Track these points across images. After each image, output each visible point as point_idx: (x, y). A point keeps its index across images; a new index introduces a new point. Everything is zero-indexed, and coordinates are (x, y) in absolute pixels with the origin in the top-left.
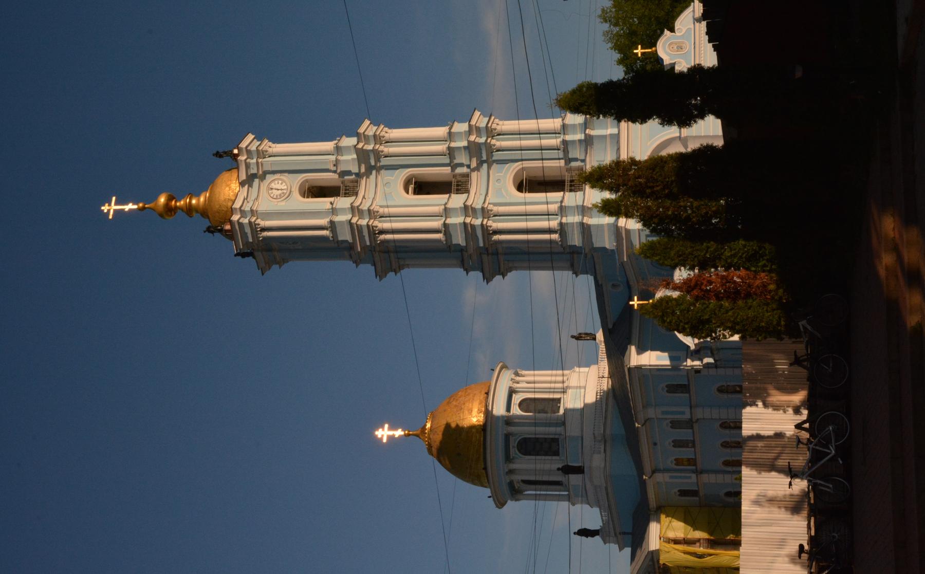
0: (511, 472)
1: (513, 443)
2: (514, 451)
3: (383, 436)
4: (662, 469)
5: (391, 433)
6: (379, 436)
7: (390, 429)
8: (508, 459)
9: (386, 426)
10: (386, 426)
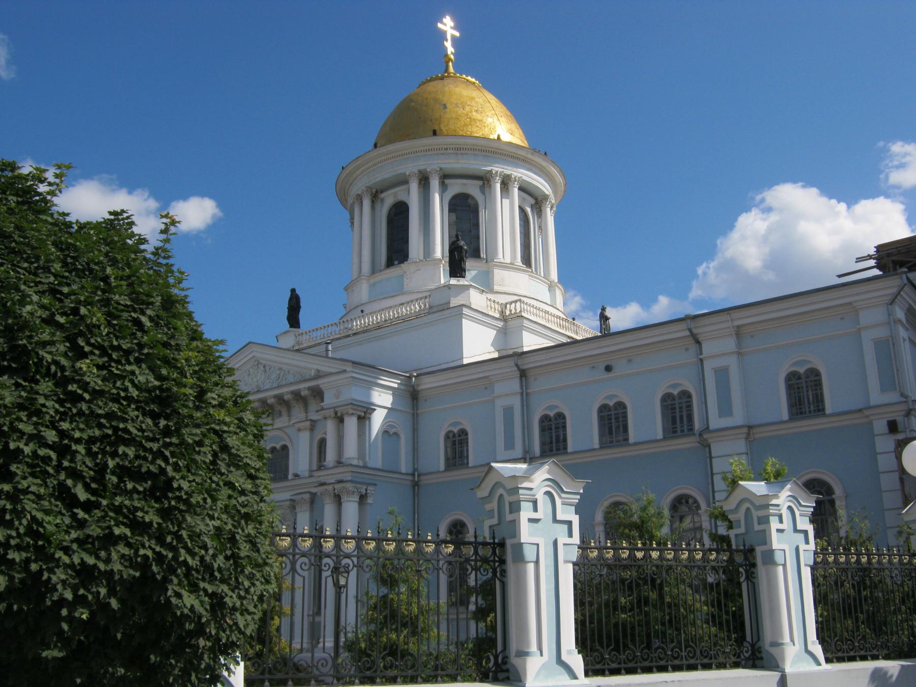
0: (424, 180)
1: (472, 187)
2: (456, 187)
3: (445, 25)
4: (528, 391)
5: (449, 37)
6: (444, 20)
7: (453, 37)
8: (446, 177)
9: (457, 34)
10: (457, 34)
